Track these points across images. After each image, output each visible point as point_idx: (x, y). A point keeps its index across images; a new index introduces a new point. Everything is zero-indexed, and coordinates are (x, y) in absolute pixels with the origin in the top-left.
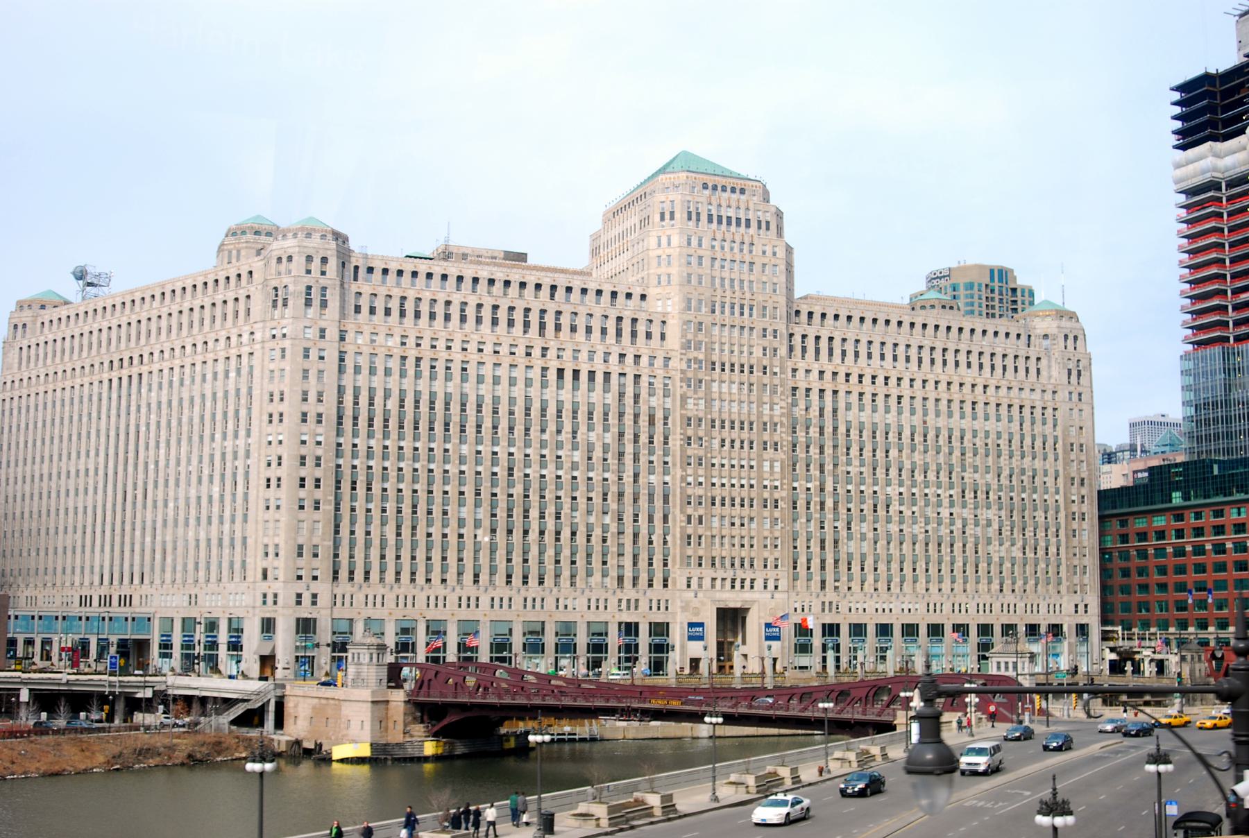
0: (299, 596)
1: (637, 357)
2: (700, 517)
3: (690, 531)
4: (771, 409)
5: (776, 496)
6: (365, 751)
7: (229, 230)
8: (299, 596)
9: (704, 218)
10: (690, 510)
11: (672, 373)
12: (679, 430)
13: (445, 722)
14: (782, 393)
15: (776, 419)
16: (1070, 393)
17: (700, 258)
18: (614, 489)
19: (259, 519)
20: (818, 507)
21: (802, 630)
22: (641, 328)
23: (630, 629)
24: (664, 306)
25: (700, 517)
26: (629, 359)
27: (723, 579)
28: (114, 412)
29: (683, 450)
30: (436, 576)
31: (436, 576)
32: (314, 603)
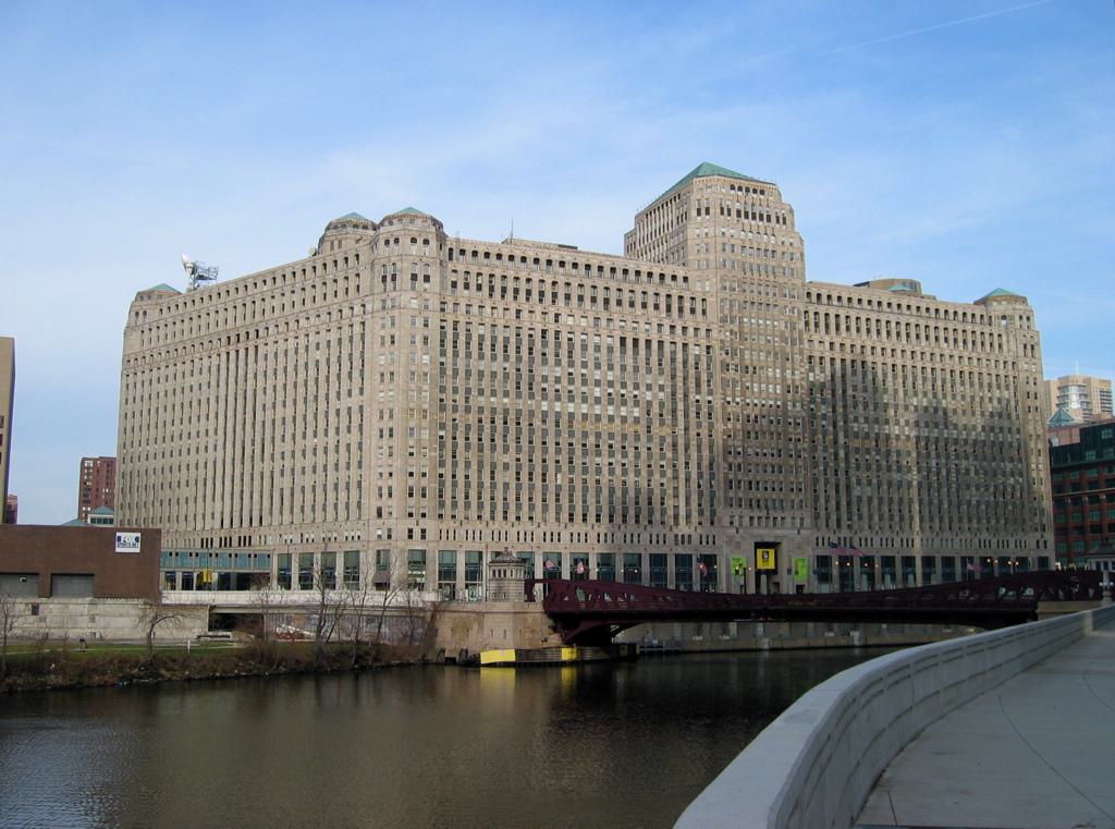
0: (410, 531)
1: (684, 329)
2: (740, 465)
3: (731, 476)
4: (793, 374)
5: (799, 447)
6: (510, 656)
7: (330, 224)
8: (410, 531)
10: (731, 459)
11: (713, 343)
13: (578, 630)
14: (802, 361)
15: (797, 383)
17: (733, 246)
18: (669, 440)
19: (372, 464)
20: (833, 458)
21: (823, 561)
22: (687, 305)
23: (684, 560)
24: (703, 287)
25: (740, 465)
26: (679, 330)
27: (759, 518)
28: (232, 380)
29: (724, 408)
30: (525, 513)
31: (525, 513)
32: (423, 537)
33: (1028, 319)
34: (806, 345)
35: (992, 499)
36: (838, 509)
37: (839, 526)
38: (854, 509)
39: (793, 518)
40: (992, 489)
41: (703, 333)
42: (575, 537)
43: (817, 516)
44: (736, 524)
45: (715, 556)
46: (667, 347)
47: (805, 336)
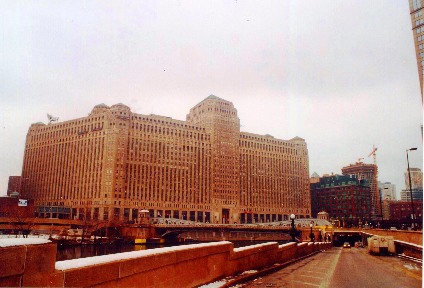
0: (115, 202)
3: (215, 188)
5: (236, 180)
7: (96, 106)
8: (115, 202)
9: (219, 110)
10: (216, 183)
12: (213, 163)
16: (304, 159)
22: (204, 137)
25: (218, 185)
26: (201, 144)
29: (214, 168)
33: (305, 145)
34: (239, 150)
35: (293, 198)
36: (247, 199)
37: (248, 204)
38: (252, 200)
39: (234, 202)
40: (293, 195)
41: (208, 145)
42: (167, 205)
43: (241, 201)
44: (217, 203)
45: (210, 212)
46: (197, 150)
47: (239, 148)
